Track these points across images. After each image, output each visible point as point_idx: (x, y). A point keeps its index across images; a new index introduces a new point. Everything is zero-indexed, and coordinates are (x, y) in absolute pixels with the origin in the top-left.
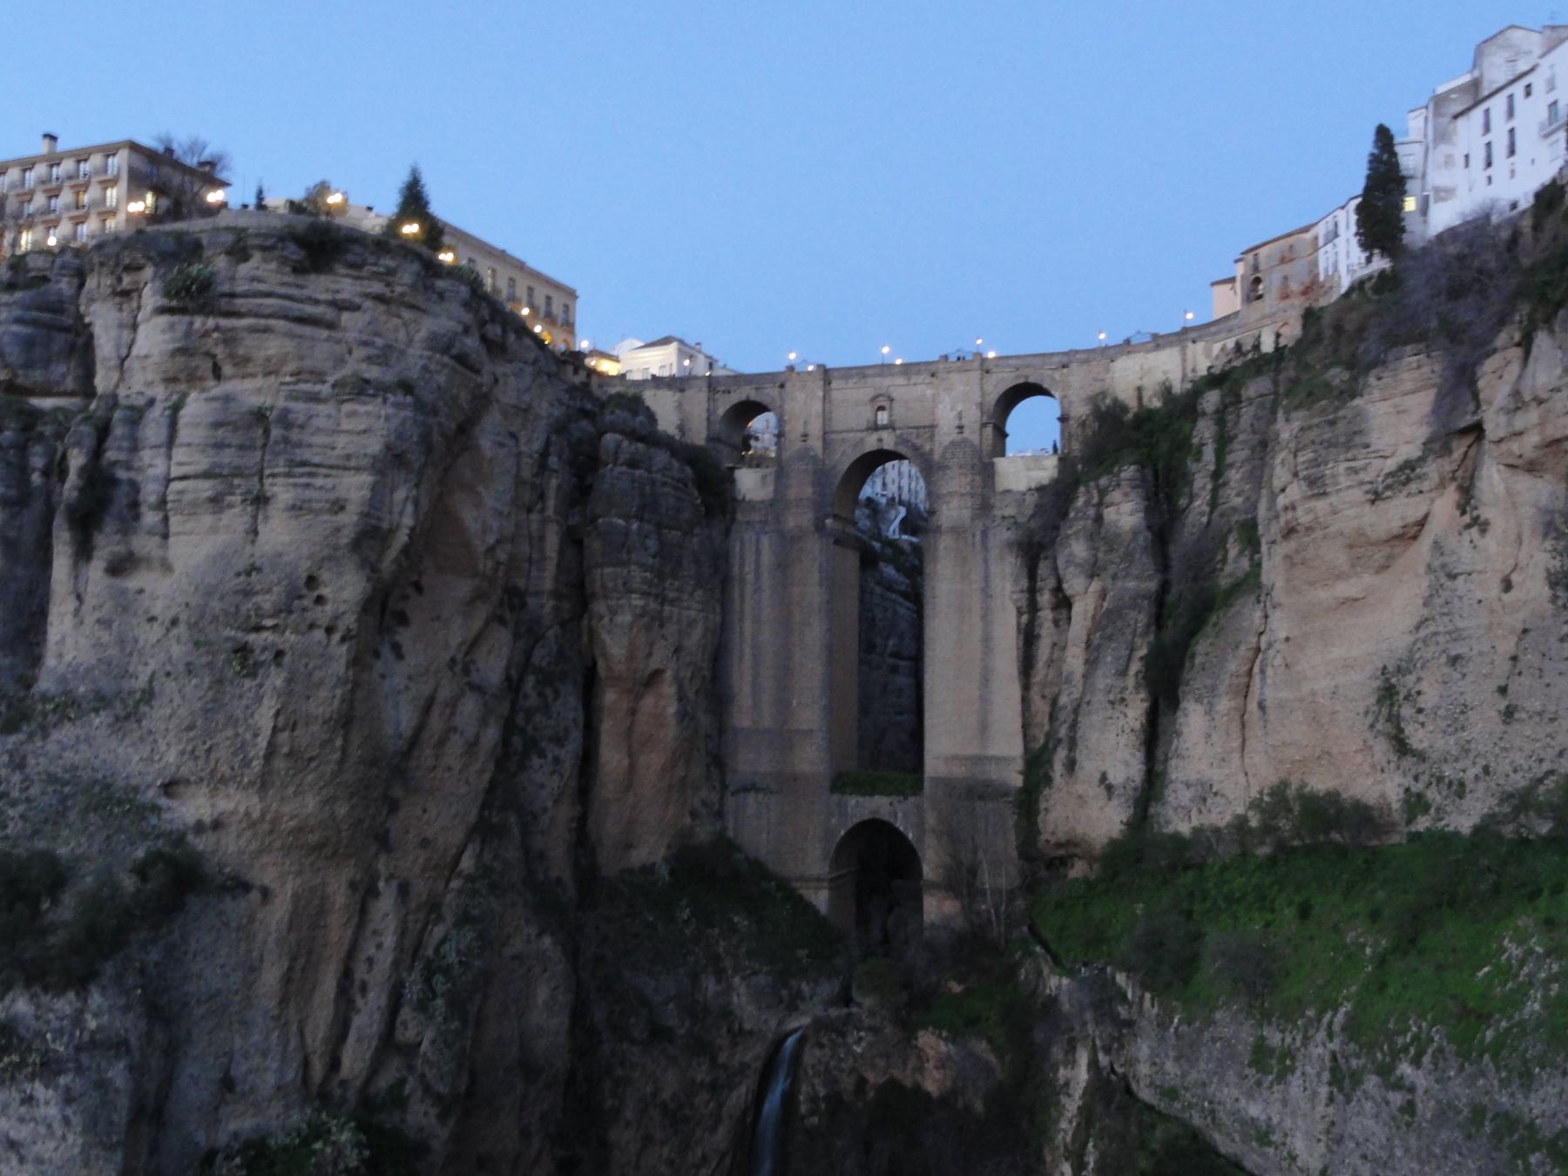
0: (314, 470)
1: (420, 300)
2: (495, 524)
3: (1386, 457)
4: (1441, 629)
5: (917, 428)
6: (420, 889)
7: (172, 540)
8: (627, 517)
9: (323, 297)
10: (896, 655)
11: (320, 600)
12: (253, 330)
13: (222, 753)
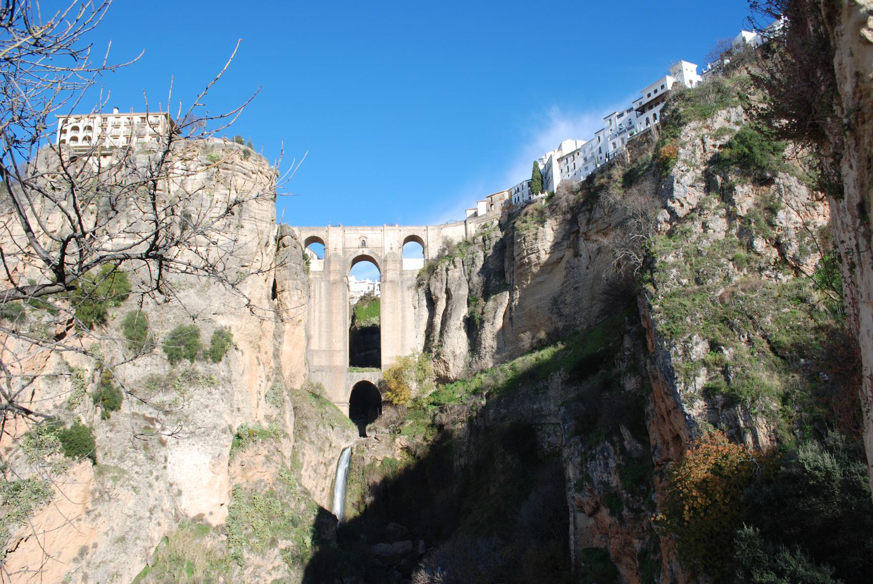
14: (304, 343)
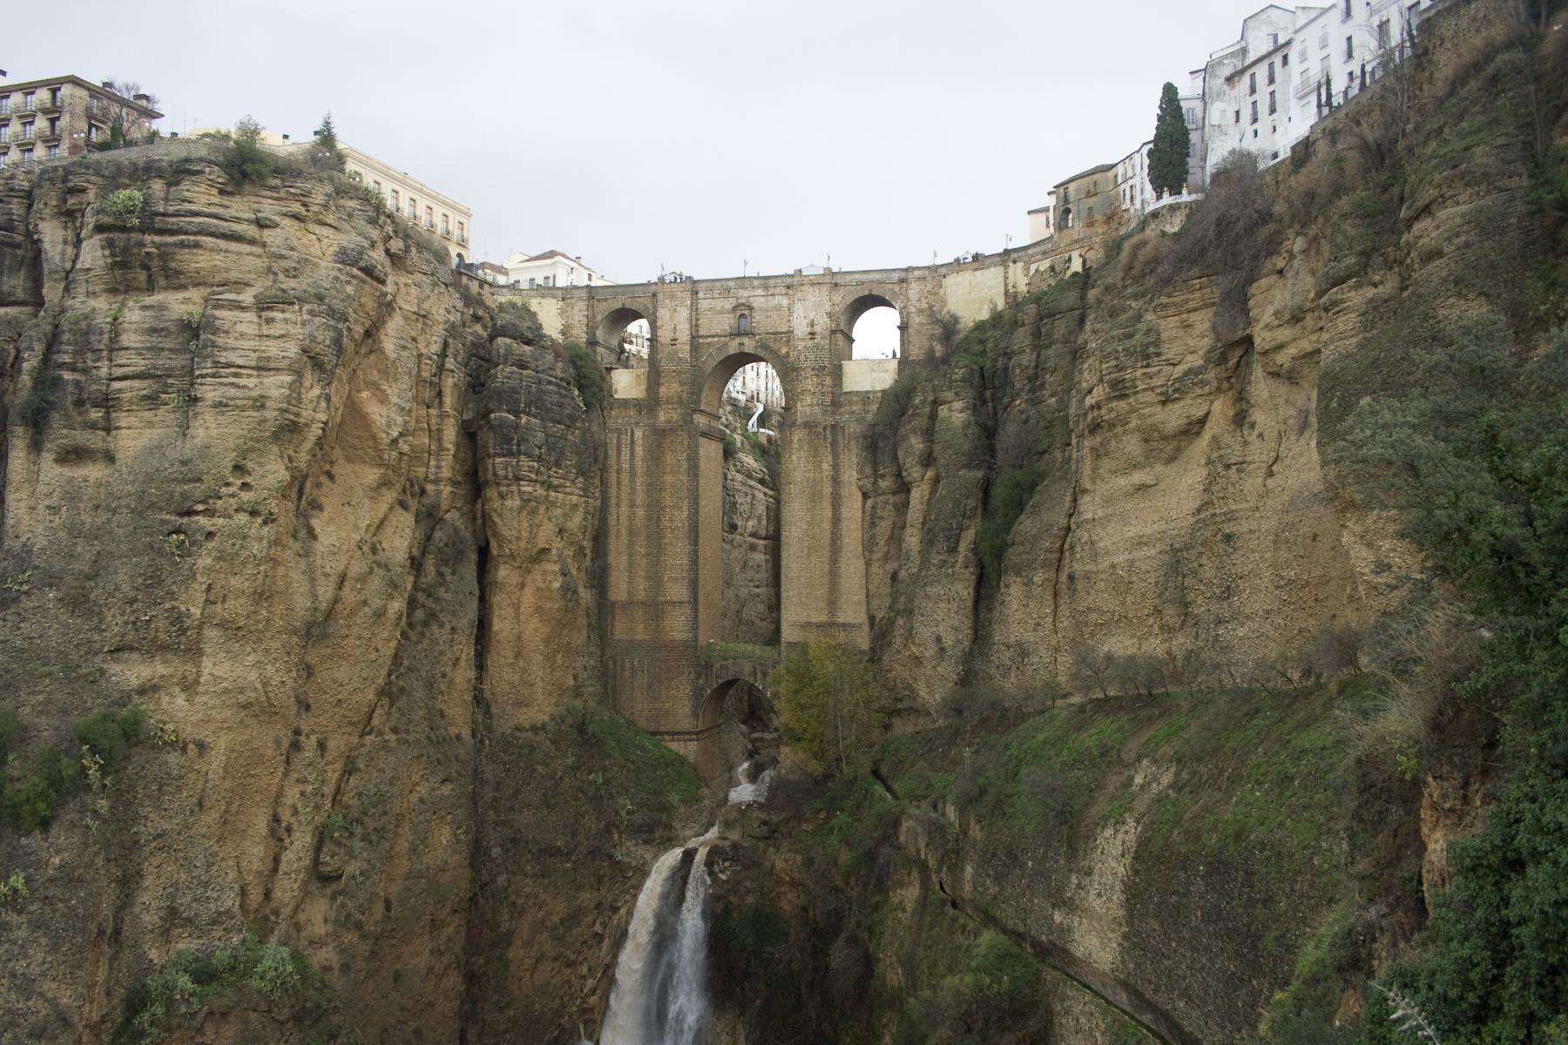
0: (239, 370)
1: (330, 218)
2: (399, 420)
3: (1174, 365)
4: (1218, 511)
5: (774, 334)
6: (336, 743)
8: (516, 413)
9: (246, 216)
10: (753, 535)
12: (182, 245)
13: (161, 624)
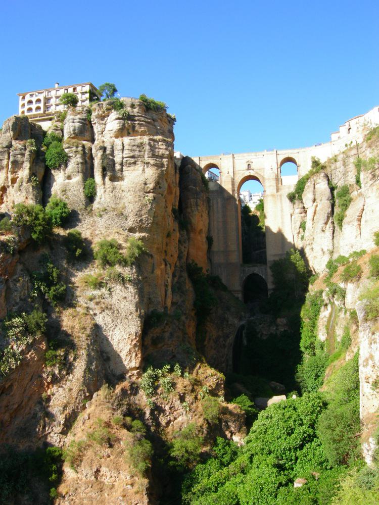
7: (124, 172)
11: (160, 187)
14: (205, 247)
